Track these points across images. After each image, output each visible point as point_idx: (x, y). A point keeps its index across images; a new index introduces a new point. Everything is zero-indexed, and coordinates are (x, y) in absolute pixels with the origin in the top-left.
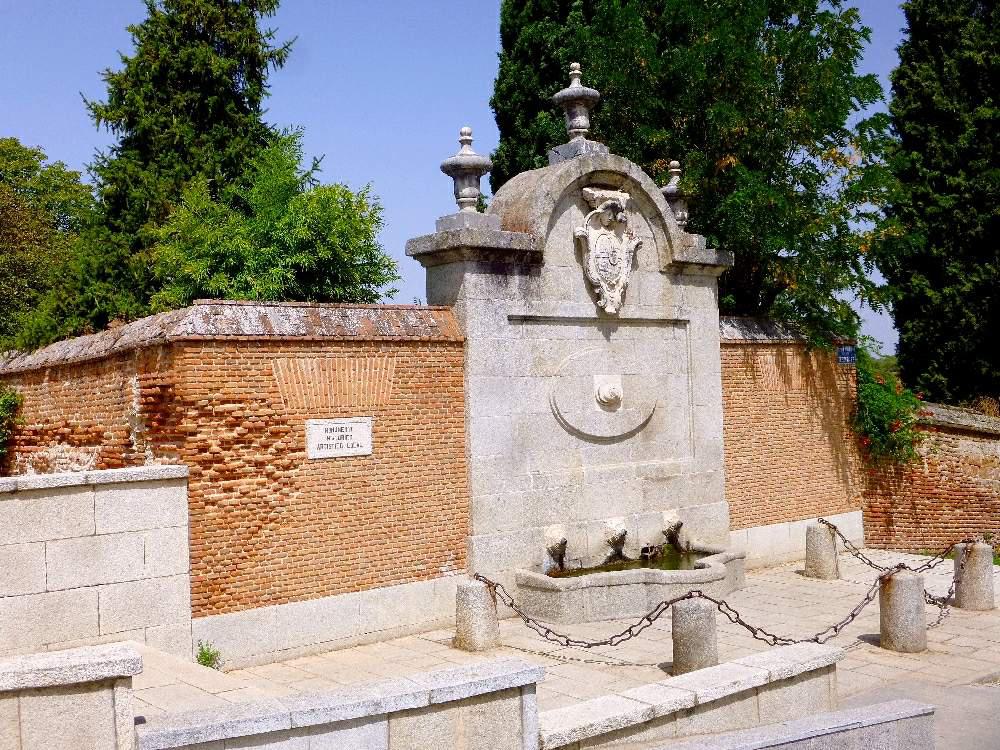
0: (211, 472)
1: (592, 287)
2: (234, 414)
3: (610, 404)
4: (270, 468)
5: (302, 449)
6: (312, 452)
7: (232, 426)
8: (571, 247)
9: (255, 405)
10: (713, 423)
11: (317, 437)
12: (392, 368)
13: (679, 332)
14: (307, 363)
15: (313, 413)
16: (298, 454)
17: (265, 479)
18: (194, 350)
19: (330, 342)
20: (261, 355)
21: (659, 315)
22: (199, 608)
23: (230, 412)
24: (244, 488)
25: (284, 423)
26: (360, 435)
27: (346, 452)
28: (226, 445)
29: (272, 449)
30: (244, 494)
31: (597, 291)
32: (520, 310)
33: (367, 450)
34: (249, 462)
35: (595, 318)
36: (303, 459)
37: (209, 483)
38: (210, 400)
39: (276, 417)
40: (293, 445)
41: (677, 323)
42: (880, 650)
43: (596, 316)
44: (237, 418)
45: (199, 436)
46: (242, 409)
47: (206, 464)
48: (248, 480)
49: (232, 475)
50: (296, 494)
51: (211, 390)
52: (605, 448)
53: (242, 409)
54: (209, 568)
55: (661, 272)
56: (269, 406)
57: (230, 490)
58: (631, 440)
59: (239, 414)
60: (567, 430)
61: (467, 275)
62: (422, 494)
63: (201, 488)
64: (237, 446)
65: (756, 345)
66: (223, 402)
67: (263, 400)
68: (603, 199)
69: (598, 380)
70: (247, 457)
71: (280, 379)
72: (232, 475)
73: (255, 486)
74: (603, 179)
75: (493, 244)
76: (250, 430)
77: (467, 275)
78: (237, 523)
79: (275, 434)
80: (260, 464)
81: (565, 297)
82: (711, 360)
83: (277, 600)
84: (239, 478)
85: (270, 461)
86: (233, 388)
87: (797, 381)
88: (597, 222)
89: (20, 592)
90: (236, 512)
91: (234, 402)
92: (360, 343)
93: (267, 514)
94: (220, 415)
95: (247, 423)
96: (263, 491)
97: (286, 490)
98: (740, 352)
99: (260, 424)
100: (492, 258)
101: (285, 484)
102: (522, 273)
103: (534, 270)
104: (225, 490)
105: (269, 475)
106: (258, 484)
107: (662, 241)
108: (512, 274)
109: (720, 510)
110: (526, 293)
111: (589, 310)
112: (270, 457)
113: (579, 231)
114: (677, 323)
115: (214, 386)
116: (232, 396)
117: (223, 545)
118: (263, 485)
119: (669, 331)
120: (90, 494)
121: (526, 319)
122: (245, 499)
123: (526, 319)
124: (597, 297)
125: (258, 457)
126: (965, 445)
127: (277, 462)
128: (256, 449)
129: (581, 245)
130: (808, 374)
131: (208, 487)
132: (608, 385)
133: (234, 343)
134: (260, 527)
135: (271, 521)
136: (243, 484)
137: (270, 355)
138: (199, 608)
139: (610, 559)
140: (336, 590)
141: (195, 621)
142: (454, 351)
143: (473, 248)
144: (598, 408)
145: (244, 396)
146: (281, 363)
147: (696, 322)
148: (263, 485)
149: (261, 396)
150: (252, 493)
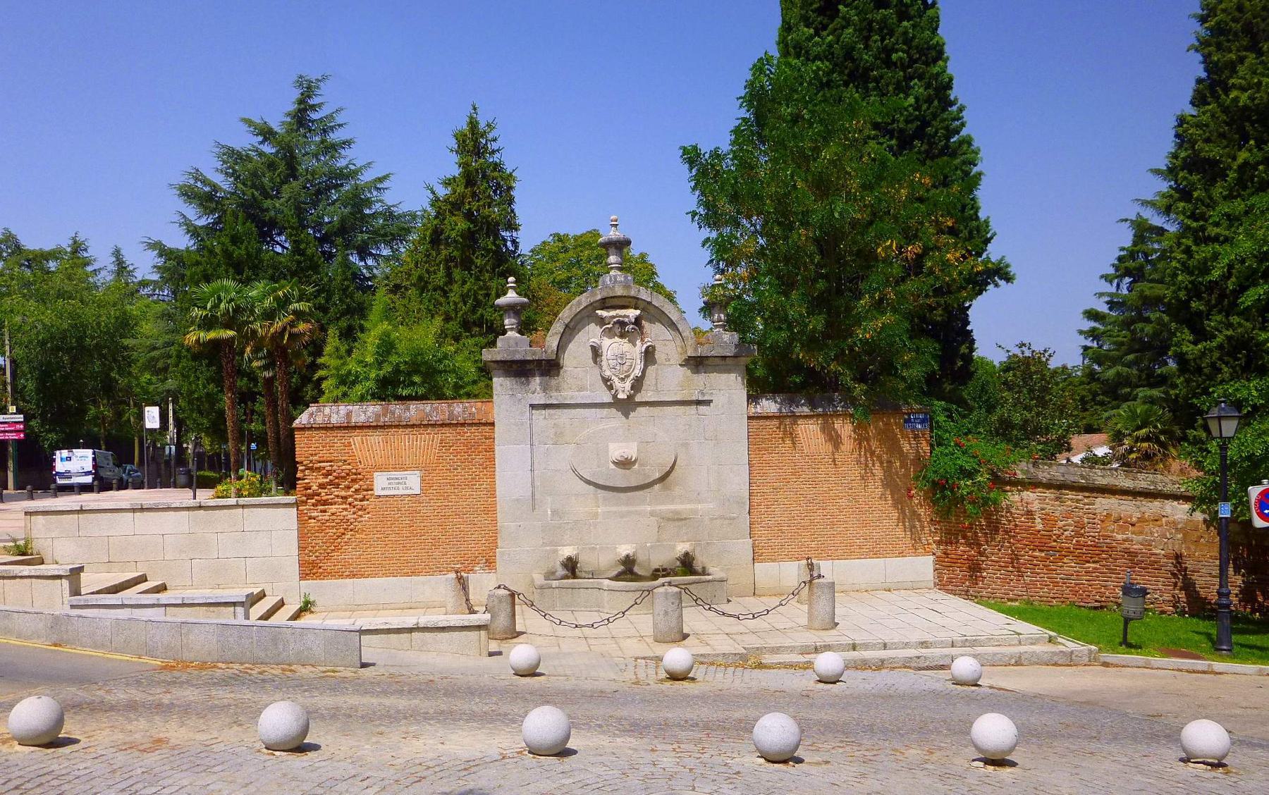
0: (313, 501)
1: (606, 381)
3: (625, 464)
4: (350, 500)
5: (372, 490)
6: (378, 492)
7: (326, 475)
8: (590, 354)
10: (738, 482)
11: (381, 483)
13: (702, 408)
14: (375, 438)
15: (381, 468)
16: (370, 492)
17: (348, 506)
19: (390, 426)
22: (304, 576)
24: (333, 511)
25: (360, 474)
26: (412, 482)
28: (322, 486)
29: (353, 489)
30: (333, 514)
31: (609, 383)
32: (539, 399)
34: (338, 496)
38: (311, 461)
39: (354, 471)
41: (699, 403)
44: (328, 471)
45: (306, 481)
47: (310, 497)
48: (337, 506)
49: (325, 503)
50: (367, 516)
51: (312, 455)
52: (622, 495)
57: (325, 511)
63: (306, 509)
64: (328, 487)
65: (795, 417)
66: (320, 462)
67: (345, 461)
69: (612, 446)
70: (336, 493)
71: (356, 450)
72: (325, 503)
74: (616, 302)
75: (509, 358)
76: (337, 478)
79: (354, 481)
80: (345, 498)
81: (581, 389)
83: (353, 575)
84: (332, 505)
85: (351, 496)
87: (848, 445)
88: (609, 333)
90: (328, 524)
92: (413, 426)
94: (319, 469)
95: (335, 474)
96: (345, 513)
97: (360, 513)
98: (775, 422)
101: (360, 510)
102: (542, 375)
104: (322, 511)
105: (350, 504)
108: (534, 376)
111: (607, 398)
112: (350, 493)
113: (595, 340)
114: (699, 403)
116: (325, 458)
118: (345, 509)
122: (334, 517)
124: (610, 388)
125: (343, 493)
126: (1103, 504)
128: (343, 489)
129: (596, 352)
130: (861, 440)
132: (618, 450)
133: (326, 429)
134: (344, 534)
136: (333, 508)
137: (349, 435)
138: (304, 576)
142: (487, 428)
144: (612, 466)
146: (356, 439)
147: (719, 399)
148: (345, 509)
150: (338, 514)
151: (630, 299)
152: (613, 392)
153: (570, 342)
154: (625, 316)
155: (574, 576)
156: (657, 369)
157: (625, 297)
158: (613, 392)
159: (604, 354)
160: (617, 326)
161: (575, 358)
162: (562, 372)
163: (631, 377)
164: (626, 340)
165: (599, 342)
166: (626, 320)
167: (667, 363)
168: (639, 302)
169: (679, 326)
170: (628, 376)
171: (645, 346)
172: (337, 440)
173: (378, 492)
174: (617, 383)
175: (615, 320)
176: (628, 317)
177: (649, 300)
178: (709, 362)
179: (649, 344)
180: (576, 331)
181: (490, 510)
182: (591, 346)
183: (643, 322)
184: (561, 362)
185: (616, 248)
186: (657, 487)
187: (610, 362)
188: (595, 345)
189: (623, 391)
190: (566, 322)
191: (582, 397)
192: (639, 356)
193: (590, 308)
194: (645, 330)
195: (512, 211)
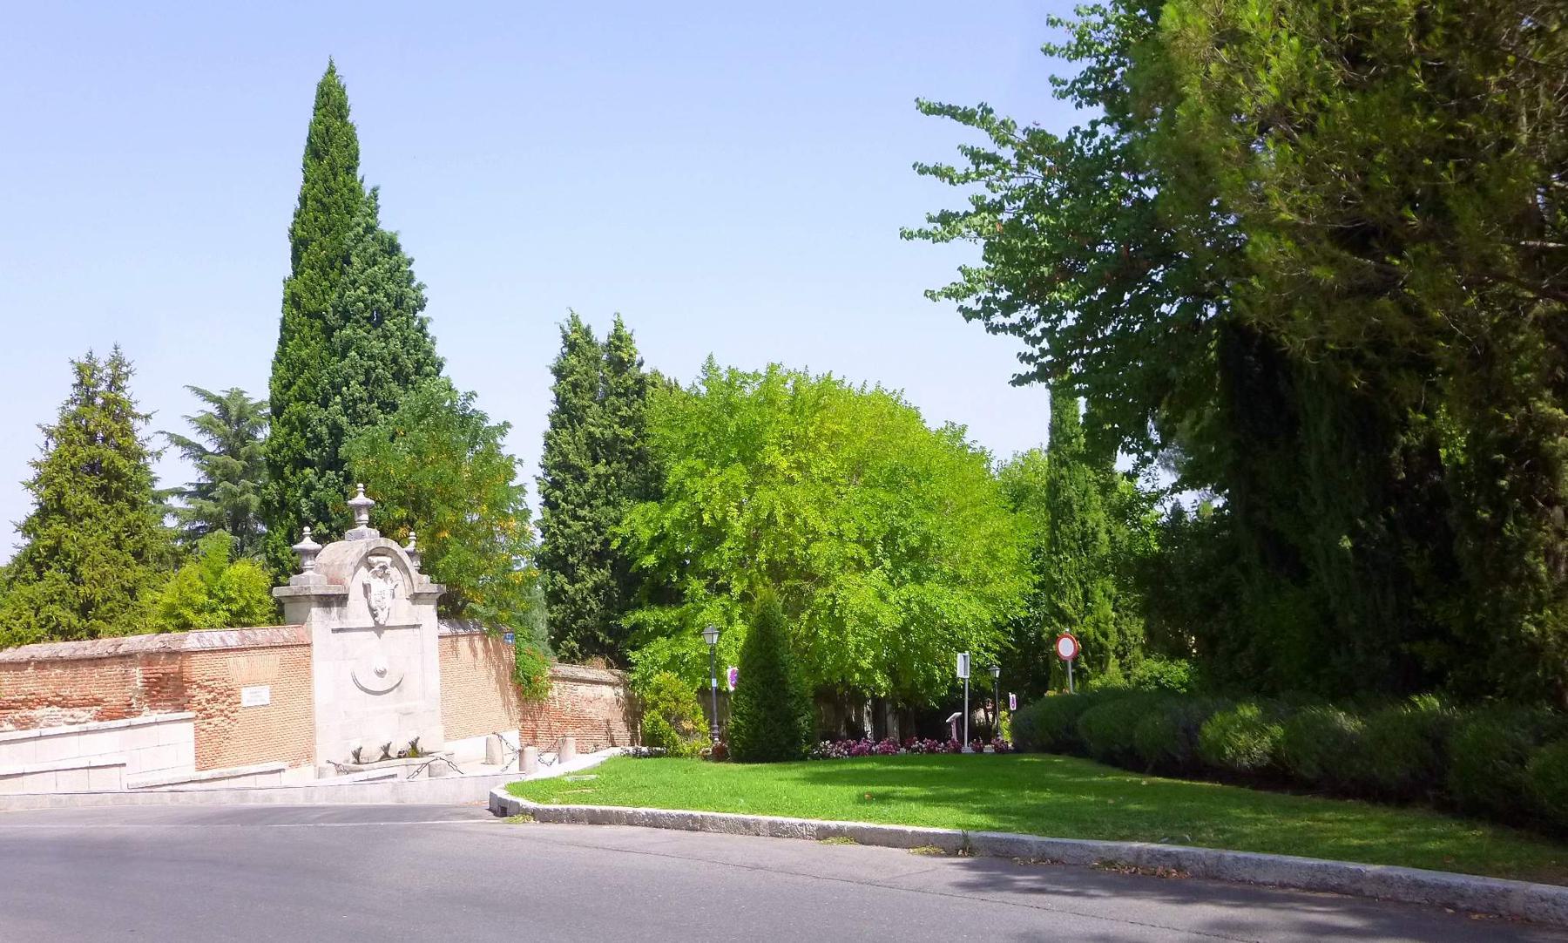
1: (372, 610)
3: (381, 674)
6: (244, 704)
7: (210, 692)
10: (434, 681)
11: (248, 697)
14: (242, 659)
28: (208, 701)
41: (414, 626)
65: (457, 635)
74: (378, 551)
75: (325, 593)
79: (229, 696)
80: (222, 711)
81: (358, 617)
87: (481, 655)
96: (223, 724)
98: (449, 640)
102: (338, 606)
107: (407, 581)
109: (439, 731)
111: (371, 623)
114: (414, 626)
120: (156, 726)
124: (374, 616)
126: (583, 689)
129: (367, 588)
130: (487, 650)
133: (211, 651)
136: (215, 720)
144: (375, 676)
146: (231, 659)
155: (359, 763)
172: (218, 660)
173: (244, 704)
178: (421, 597)
181: (309, 714)
186: (396, 690)
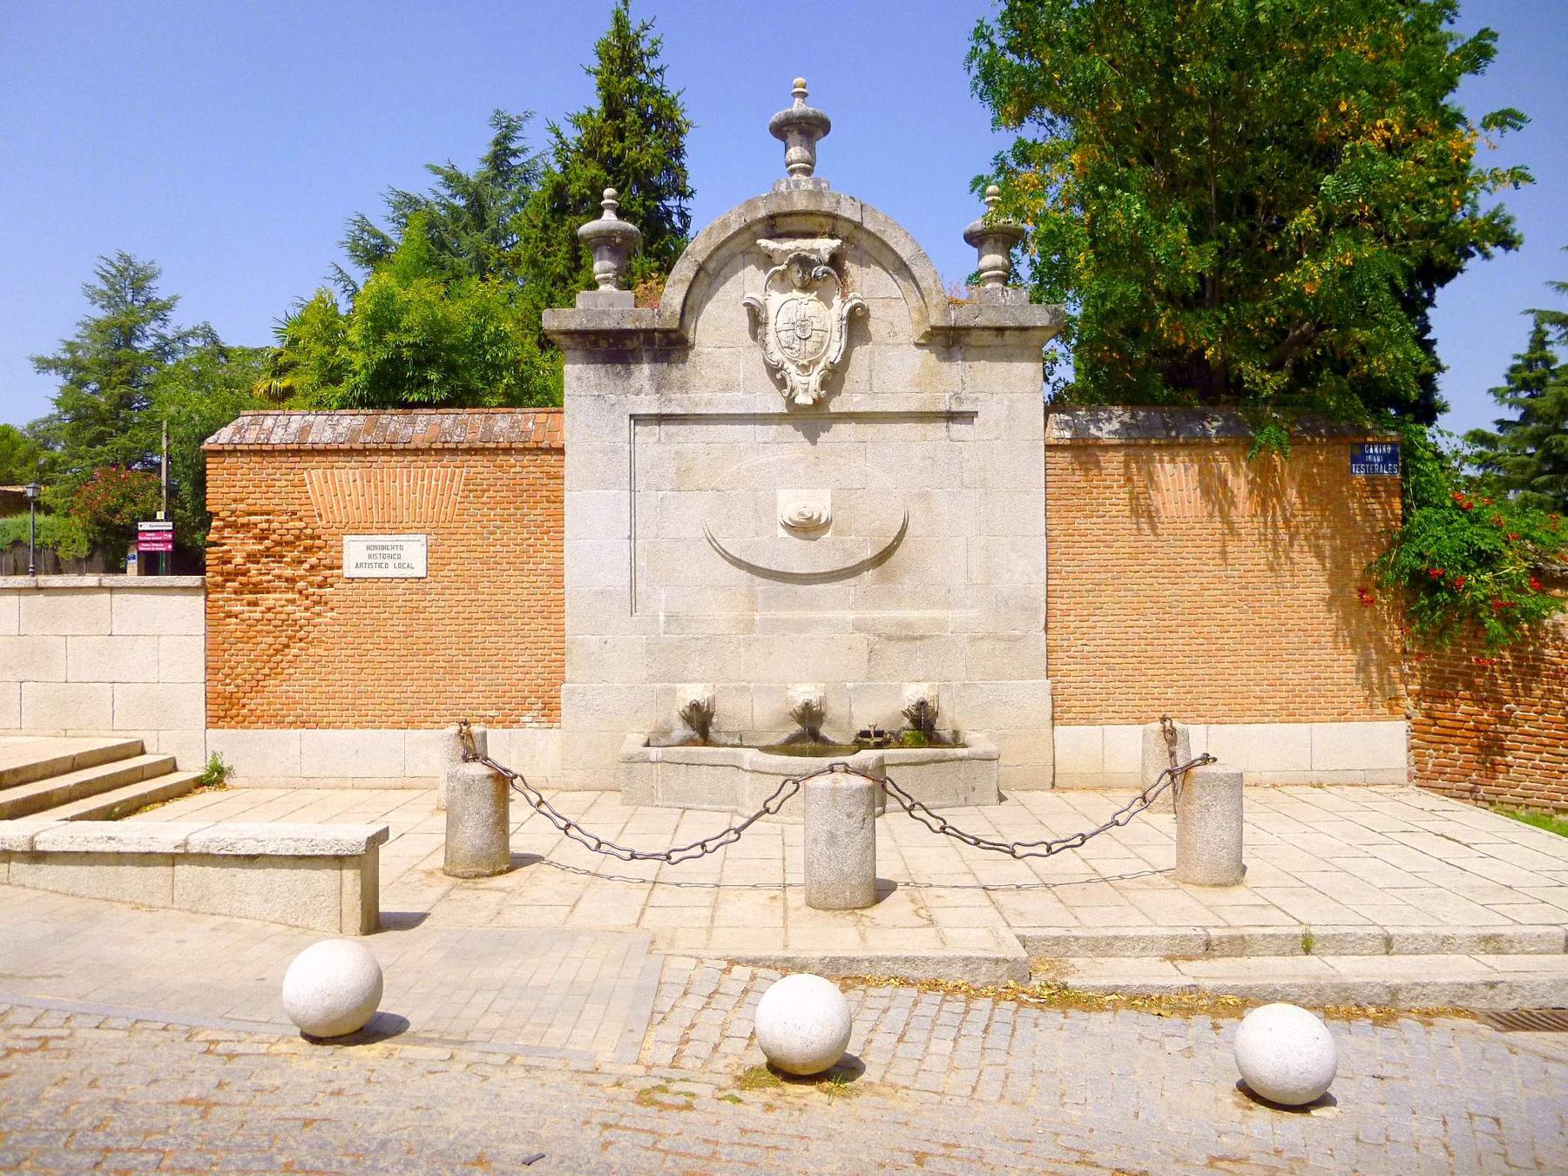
0: (236, 584)
1: (774, 370)
2: (260, 526)
3: (807, 529)
4: (301, 584)
5: (340, 567)
6: (349, 570)
7: (262, 539)
8: (745, 321)
9: (285, 518)
11: (356, 555)
12: (458, 484)
13: (958, 429)
14: (348, 474)
15: (359, 529)
16: (336, 572)
17: (297, 596)
18: (216, 460)
19: (376, 451)
20: (292, 465)
21: (913, 406)
22: (214, 721)
23: (256, 524)
24: (270, 603)
25: (319, 538)
26: (413, 554)
27: (391, 572)
28: (252, 558)
29: (306, 566)
30: (269, 610)
31: (778, 376)
32: (648, 404)
33: (420, 571)
34: (279, 577)
35: (783, 414)
36: (339, 577)
37: (233, 596)
38: (233, 512)
39: (308, 531)
40: (328, 562)
41: (951, 417)
42: (1462, 979)
43: (786, 411)
44: (262, 530)
45: (225, 548)
46: (267, 521)
47: (229, 576)
48: (278, 596)
49: (257, 589)
50: (329, 614)
51: (235, 501)
52: (803, 589)
53: (267, 521)
54: (228, 681)
55: (917, 345)
56: (301, 520)
57: (255, 604)
58: (852, 581)
59: (265, 526)
60: (730, 562)
61: (567, 368)
62: (496, 627)
63: (222, 599)
64: (264, 560)
66: (250, 514)
67: (294, 513)
68: (786, 253)
69: (783, 495)
70: (277, 572)
71: (313, 490)
72: (257, 589)
73: (283, 603)
75: (591, 326)
76: (278, 544)
77: (567, 368)
78: (259, 639)
80: (291, 580)
81: (727, 387)
82: (1031, 466)
83: (304, 724)
84: (268, 592)
85: (302, 578)
86: (259, 500)
87: (1244, 506)
88: (781, 281)
89: (44, 679)
90: (259, 628)
91: (262, 514)
92: (417, 451)
93: (292, 634)
94: (246, 526)
95: (275, 537)
96: (290, 608)
97: (317, 609)
99: (289, 538)
100: (603, 343)
101: (316, 603)
102: (655, 360)
103: (675, 356)
104: (249, 604)
105: (300, 592)
106: (287, 600)
107: (914, 299)
108: (638, 361)
109: (1034, 694)
110: (659, 387)
111: (776, 404)
112: (302, 572)
113: (755, 295)
114: (951, 417)
115: (238, 496)
116: (257, 508)
117: (241, 659)
118: (292, 601)
119: (938, 430)
120: (106, 596)
121: (661, 419)
122: (270, 615)
123: (661, 419)
124: (782, 384)
125: (288, 572)
127: (311, 579)
128: (288, 564)
129: (756, 318)
131: (230, 600)
132: (793, 503)
134: (287, 646)
135: (301, 640)
136: (269, 600)
137: (303, 465)
138: (214, 721)
139: (793, 739)
140: (374, 724)
141: (210, 731)
142: (551, 459)
143: (569, 333)
144: (782, 533)
145: (271, 508)
146: (315, 475)
147: (990, 411)
148: (292, 601)
149: (291, 508)
150: (279, 609)
151: (822, 219)
152: (787, 391)
153: (709, 298)
154: (813, 251)
155: (706, 740)
156: (872, 353)
157: (812, 213)
158: (787, 391)
159: (772, 320)
160: (796, 267)
161: (717, 329)
162: (691, 353)
163: (822, 365)
164: (813, 296)
165: (761, 300)
166: (814, 257)
167: (891, 341)
168: (840, 224)
169: (914, 269)
170: (815, 363)
171: (848, 306)
172: (279, 474)
173: (349, 570)
174: (793, 375)
175: (791, 256)
176: (817, 251)
177: (857, 218)
178: (974, 338)
179: (855, 302)
180: (721, 279)
181: (553, 610)
182: (746, 304)
183: (847, 264)
184: (691, 336)
185: (801, 132)
186: (868, 575)
187: (783, 335)
188: (753, 302)
189: (806, 391)
190: (700, 260)
191: (729, 403)
192: (836, 327)
193: (747, 235)
194: (849, 280)
195: (682, 165)
